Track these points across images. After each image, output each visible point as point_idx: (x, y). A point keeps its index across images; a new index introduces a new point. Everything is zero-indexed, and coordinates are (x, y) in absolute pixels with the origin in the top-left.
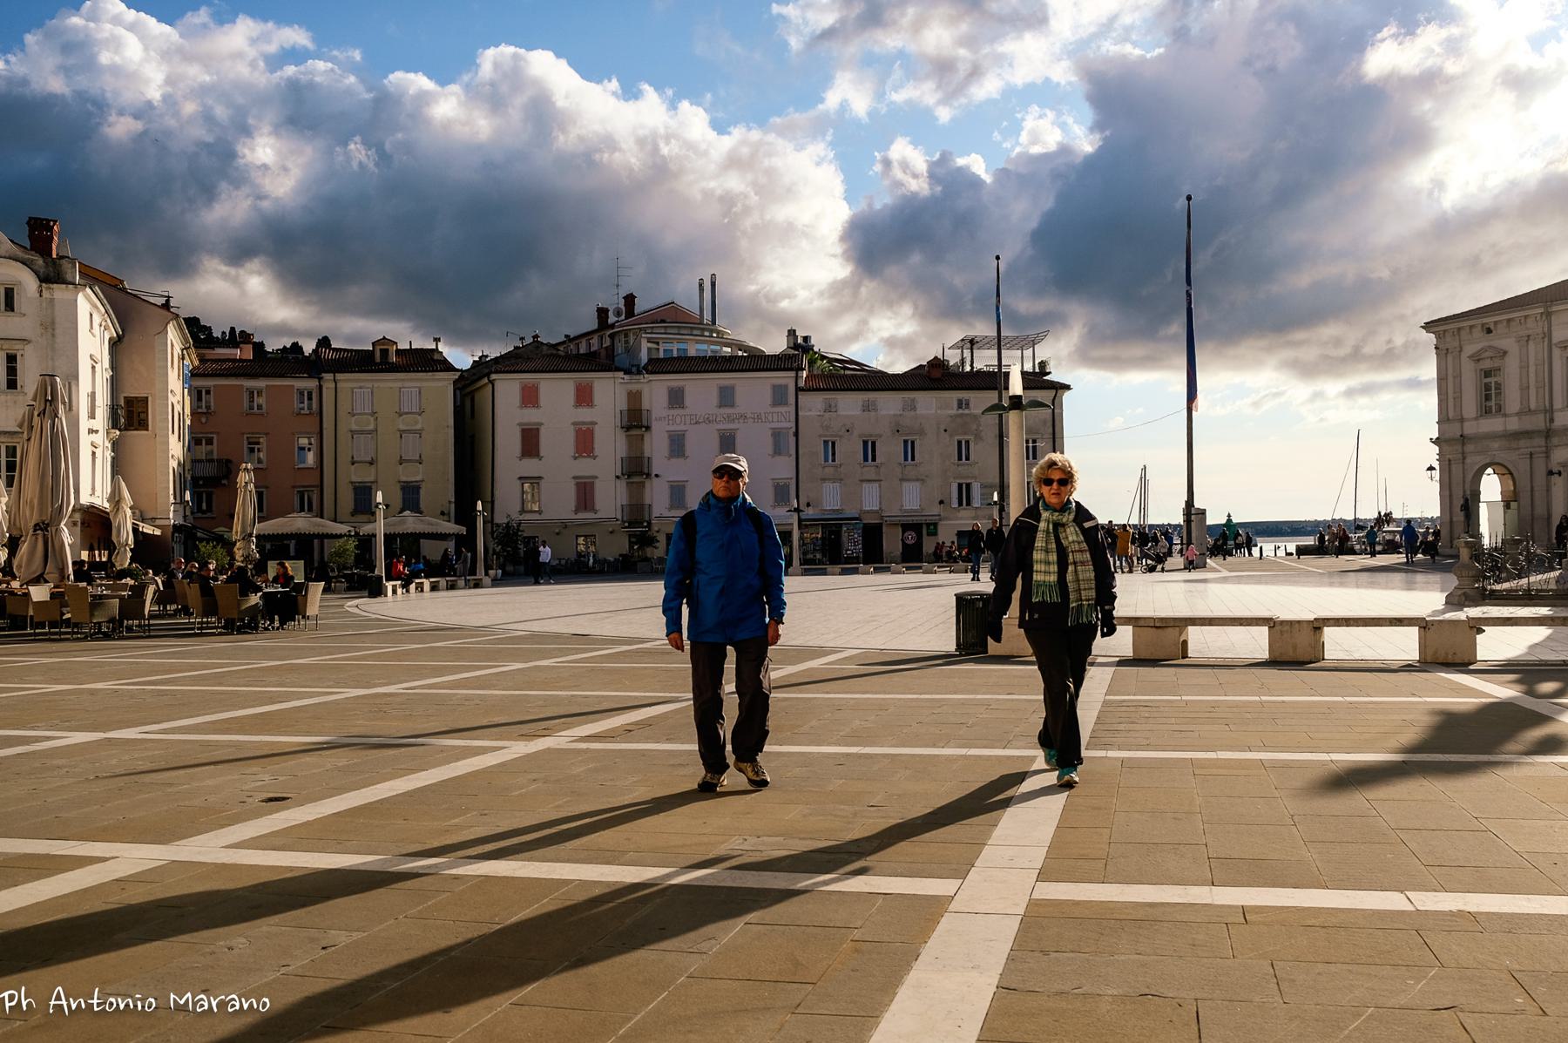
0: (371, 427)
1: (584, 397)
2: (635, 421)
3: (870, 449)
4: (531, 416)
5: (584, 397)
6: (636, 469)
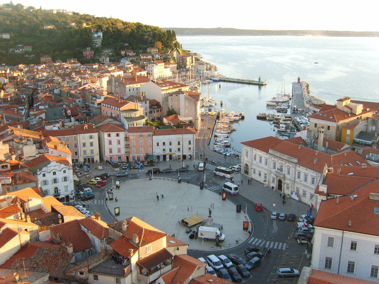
1: (118, 135)
2: (127, 139)
6: (127, 146)
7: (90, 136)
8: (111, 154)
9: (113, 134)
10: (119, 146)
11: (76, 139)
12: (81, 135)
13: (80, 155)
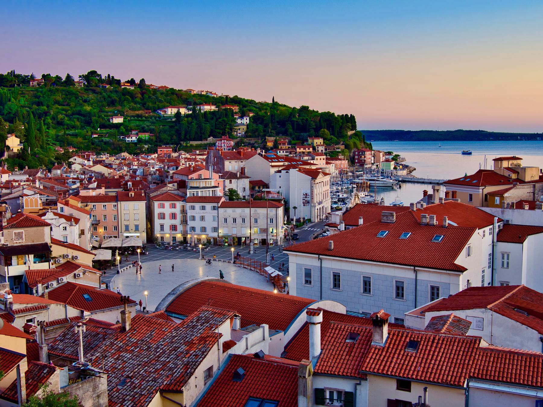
1: (174, 206)
2: (184, 211)
3: (235, 220)
4: (162, 210)
12: (123, 203)
13: (120, 231)
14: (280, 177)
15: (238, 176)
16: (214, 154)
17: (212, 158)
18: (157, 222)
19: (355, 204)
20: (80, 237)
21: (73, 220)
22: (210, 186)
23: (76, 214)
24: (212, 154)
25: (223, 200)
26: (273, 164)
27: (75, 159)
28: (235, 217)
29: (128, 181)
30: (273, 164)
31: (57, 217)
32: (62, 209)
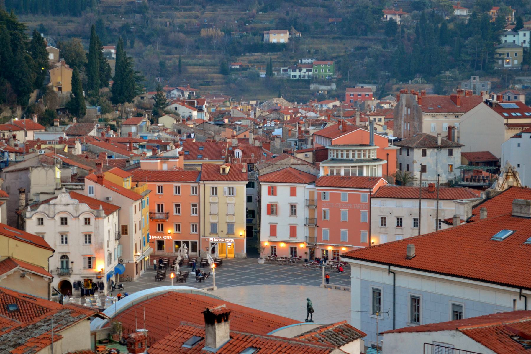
0: (217, 201)
1: (293, 193)
5: (293, 193)
6: (312, 223)
7: (229, 188)
8: (273, 239)
9: (283, 190)
10: (293, 221)
11: (195, 190)
12: (209, 185)
14: (519, 145)
15: (439, 142)
16: (407, 100)
17: (405, 109)
18: (266, 220)
19: (506, 187)
20: (118, 238)
21: (101, 208)
22: (367, 158)
23: (115, 198)
24: (404, 102)
25: (382, 182)
26: (511, 121)
27: (176, 108)
28: (400, 215)
29: (235, 147)
30: (511, 121)
31: (76, 201)
32: (91, 190)
